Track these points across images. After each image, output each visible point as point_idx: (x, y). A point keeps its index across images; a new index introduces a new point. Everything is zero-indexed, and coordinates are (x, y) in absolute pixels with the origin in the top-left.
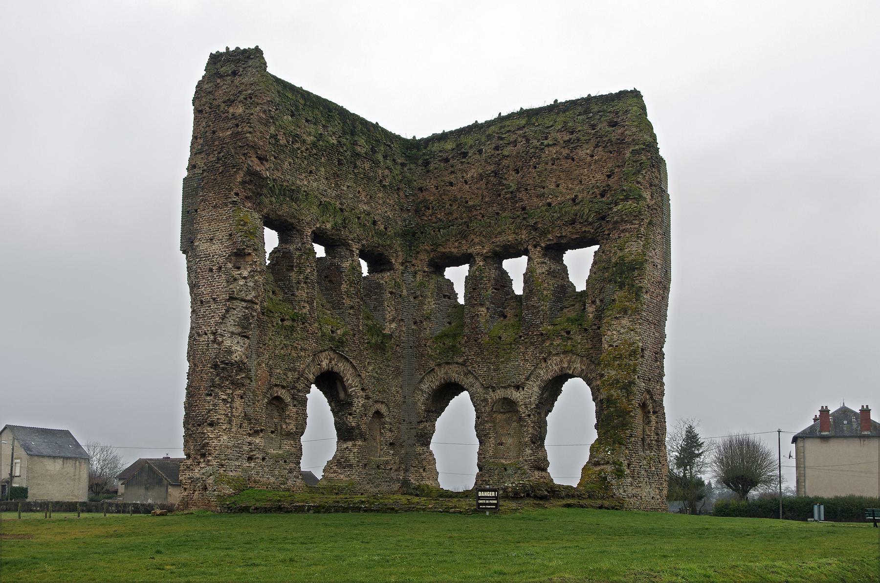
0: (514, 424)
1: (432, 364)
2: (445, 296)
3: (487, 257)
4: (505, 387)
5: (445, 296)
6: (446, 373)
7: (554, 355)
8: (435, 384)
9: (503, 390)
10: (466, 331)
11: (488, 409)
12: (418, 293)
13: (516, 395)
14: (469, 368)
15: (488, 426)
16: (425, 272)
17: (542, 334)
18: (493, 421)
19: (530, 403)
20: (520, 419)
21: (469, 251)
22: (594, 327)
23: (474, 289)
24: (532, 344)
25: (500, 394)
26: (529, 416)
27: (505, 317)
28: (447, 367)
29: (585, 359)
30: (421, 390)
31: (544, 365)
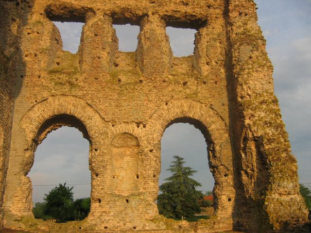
1: (45, 94)
2: (56, 40)
3: (105, 14)
5: (56, 40)
6: (60, 105)
7: (175, 99)
8: (47, 115)
9: (123, 125)
10: (85, 67)
12: (35, 29)
13: (138, 132)
14: (89, 102)
15: (106, 158)
16: (41, 14)
17: (164, 81)
19: (153, 139)
20: (141, 153)
21: (89, 6)
22: (212, 81)
23: (96, 35)
24: (155, 87)
25: (121, 128)
26: (151, 151)
27: (116, 65)
28: (62, 99)
29: (204, 105)
30: (29, 118)
31: (165, 107)
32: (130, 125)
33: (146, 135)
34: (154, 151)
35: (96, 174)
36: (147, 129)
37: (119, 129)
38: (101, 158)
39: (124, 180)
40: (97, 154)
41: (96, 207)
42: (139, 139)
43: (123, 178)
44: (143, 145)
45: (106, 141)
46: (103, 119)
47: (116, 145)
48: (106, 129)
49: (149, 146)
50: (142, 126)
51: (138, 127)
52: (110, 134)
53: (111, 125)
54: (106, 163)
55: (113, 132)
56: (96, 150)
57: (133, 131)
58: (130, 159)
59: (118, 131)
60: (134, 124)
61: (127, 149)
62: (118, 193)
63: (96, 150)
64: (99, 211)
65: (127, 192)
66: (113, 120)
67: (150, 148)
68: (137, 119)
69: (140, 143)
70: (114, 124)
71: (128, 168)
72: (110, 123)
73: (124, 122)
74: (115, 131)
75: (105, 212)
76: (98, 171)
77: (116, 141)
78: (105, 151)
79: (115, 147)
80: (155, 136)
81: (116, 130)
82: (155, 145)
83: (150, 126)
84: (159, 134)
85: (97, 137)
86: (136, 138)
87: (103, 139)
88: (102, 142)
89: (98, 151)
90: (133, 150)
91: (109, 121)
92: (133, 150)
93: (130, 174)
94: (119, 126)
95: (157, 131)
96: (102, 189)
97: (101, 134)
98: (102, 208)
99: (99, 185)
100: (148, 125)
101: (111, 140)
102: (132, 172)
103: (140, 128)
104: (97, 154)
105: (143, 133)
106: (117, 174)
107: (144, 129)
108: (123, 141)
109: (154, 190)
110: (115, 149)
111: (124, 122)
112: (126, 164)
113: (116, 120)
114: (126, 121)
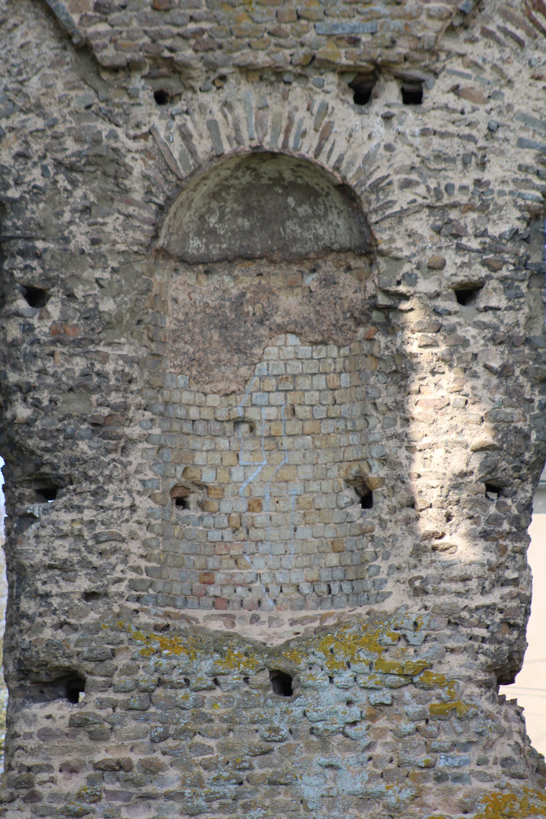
0: (283, 352)
4: (274, 76)
11: (121, 230)
15: (118, 354)
18: (142, 320)
19: (482, 200)
25: (226, 119)
26: (466, 294)
32: (297, 91)
33: (422, 167)
34: (493, 297)
35: (42, 479)
36: (435, 120)
37: (213, 126)
38: (79, 364)
39: (260, 518)
40: (42, 328)
41: (46, 734)
42: (371, 203)
43: (255, 505)
44: (402, 247)
45: (112, 223)
46: (85, 49)
47: (195, 246)
48: (103, 127)
49: (452, 258)
50: (390, 93)
51: (363, 96)
52: (138, 167)
53: (146, 96)
54: (115, 398)
55: (159, 155)
56: (36, 297)
57: (324, 138)
58: (306, 350)
59: (203, 146)
60: (331, 78)
61: (276, 278)
62: (217, 626)
63: (36, 297)
64: (71, 758)
65: (287, 615)
66: (157, 60)
67: (457, 268)
68: (354, 41)
69: (382, 237)
70: (172, 85)
71: (293, 427)
72: (137, 82)
73: (247, 70)
74: (177, 148)
75: (118, 767)
76: (58, 462)
77: (188, 217)
78: (108, 306)
79: (187, 262)
80: (494, 173)
81: (186, 136)
82: (495, 246)
83: (456, 90)
84: (529, 158)
85: (37, 192)
86: (345, 190)
87: (86, 210)
88: (80, 237)
89: (54, 308)
90: (329, 282)
91: (131, 67)
92: (329, 282)
93: (307, 471)
94: (211, 100)
95: (515, 130)
96: (89, 596)
97: (72, 168)
98: (95, 737)
99: (64, 568)
100: (444, 82)
101: (148, 214)
102: (325, 458)
103: (378, 107)
104: (42, 328)
105: (404, 156)
106: (208, 477)
107: (410, 111)
108: (247, 212)
109: (494, 597)
110: (187, 277)
111: (247, 70)
112: (278, 398)
113: (187, 54)
114: (262, 58)
